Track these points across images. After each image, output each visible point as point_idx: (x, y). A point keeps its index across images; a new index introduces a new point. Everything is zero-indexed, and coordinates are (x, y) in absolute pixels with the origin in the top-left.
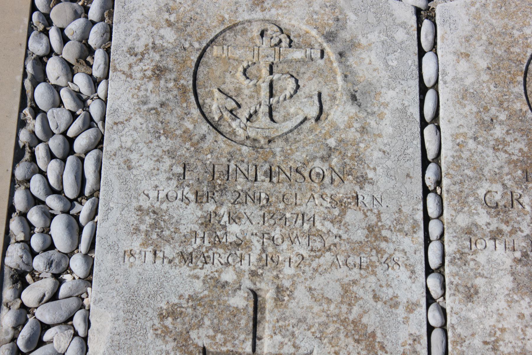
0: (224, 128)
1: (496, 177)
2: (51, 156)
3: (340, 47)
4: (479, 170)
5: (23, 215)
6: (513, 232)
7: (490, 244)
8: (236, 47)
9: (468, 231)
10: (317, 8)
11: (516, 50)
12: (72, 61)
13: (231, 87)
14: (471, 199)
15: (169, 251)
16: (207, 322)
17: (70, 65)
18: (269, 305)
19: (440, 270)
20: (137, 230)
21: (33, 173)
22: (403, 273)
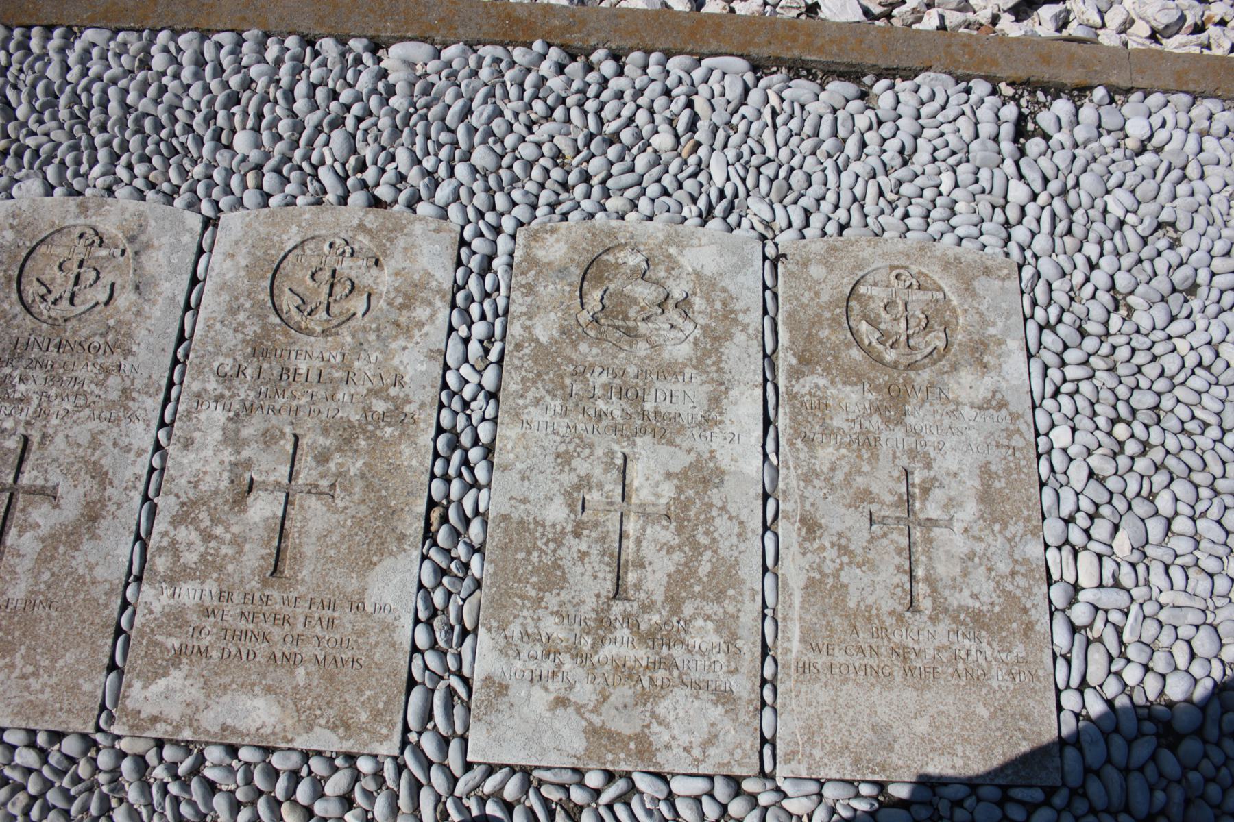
0: (35, 310)
1: (231, 353)
3: (137, 246)
4: (218, 347)
6: (232, 396)
7: (213, 405)
9: (198, 395)
13: (48, 277)
14: (207, 369)
18: (35, 447)
22: (140, 426)
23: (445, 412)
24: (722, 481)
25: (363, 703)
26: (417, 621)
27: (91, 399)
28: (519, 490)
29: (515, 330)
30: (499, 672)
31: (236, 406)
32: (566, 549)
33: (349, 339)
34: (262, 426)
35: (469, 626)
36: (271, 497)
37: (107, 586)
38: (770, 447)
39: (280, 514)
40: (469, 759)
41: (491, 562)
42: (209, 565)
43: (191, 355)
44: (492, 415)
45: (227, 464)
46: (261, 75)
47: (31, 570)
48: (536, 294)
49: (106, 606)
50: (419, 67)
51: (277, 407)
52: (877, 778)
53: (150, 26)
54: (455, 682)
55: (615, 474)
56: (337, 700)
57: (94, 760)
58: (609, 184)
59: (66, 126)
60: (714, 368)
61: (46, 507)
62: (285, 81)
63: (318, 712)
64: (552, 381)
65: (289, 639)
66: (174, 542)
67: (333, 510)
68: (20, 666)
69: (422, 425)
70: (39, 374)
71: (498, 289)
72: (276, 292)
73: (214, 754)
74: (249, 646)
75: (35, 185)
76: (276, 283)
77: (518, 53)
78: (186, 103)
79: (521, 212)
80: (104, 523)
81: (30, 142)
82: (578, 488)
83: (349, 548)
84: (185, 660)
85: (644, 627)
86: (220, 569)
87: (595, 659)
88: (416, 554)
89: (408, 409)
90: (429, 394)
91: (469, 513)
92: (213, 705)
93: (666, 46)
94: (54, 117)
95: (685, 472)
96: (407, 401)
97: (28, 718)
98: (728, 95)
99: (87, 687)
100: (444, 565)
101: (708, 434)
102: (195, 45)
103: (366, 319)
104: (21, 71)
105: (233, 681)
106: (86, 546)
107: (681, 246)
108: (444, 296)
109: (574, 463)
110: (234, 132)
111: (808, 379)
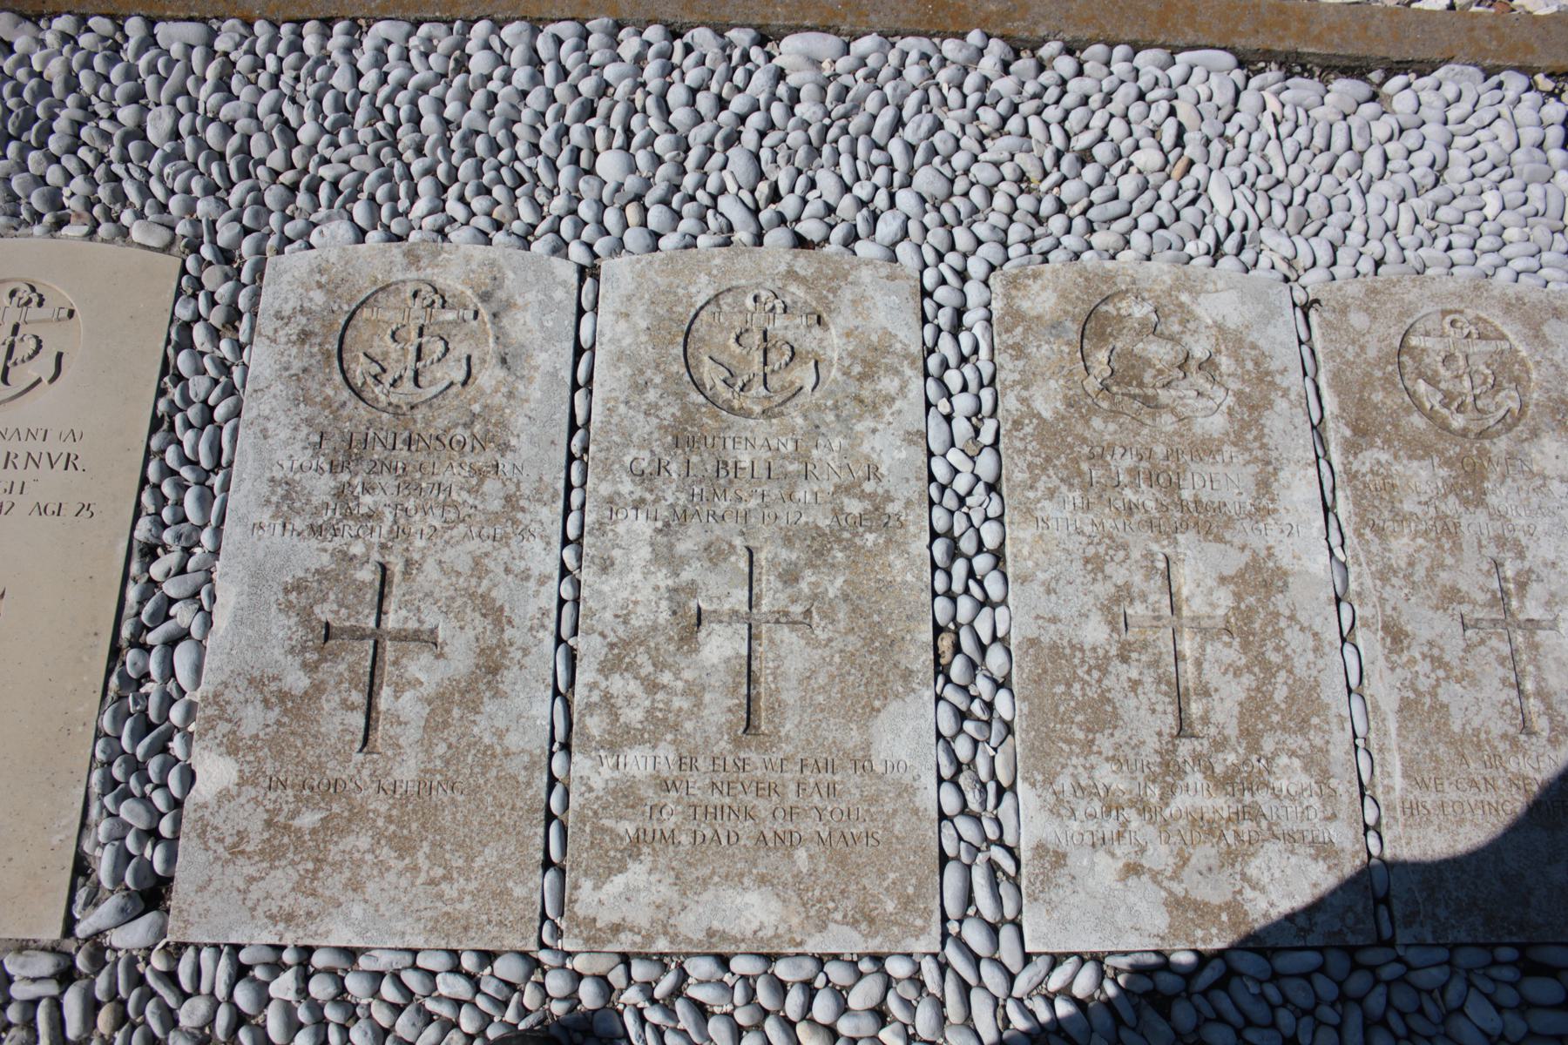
0: (367, 395)
1: (645, 443)
2: (188, 425)
3: (494, 306)
4: (627, 436)
5: (157, 487)
6: (657, 501)
7: (632, 513)
8: (387, 308)
9: (610, 501)
10: (474, 267)
11: (679, 309)
12: (219, 326)
13: (378, 351)
14: (616, 466)
15: (299, 523)
16: (332, 596)
17: (217, 330)
18: (397, 578)
19: (579, 540)
20: (268, 501)
21: (170, 443)
22: (537, 545)
23: (937, 511)
24: (1286, 584)
25: (887, 889)
26: (940, 780)
27: (464, 511)
28: (1046, 606)
29: (1010, 403)
30: (1052, 838)
31: (664, 513)
32: (1113, 678)
33: (800, 421)
34: (704, 539)
35: (1005, 783)
36: (730, 630)
37: (526, 758)
38: (1335, 539)
39: (745, 652)
40: (1028, 950)
41: (1025, 699)
42: (659, 725)
43: (592, 448)
44: (998, 513)
45: (663, 590)
46: (622, 77)
47: (420, 742)
48: (1028, 356)
49: (529, 784)
50: (826, 65)
51: (719, 512)
52: (1515, 939)
53: (462, 15)
54: (998, 854)
55: (1158, 581)
56: (853, 887)
57: (542, 985)
58: (1092, 214)
59: (370, 149)
60: (1257, 444)
61: (426, 658)
62: (654, 85)
63: (831, 905)
64: (1065, 466)
65: (779, 813)
66: (607, 697)
67: (813, 643)
68: (425, 868)
69: (912, 529)
70: (387, 480)
71: (976, 351)
72: (691, 361)
73: (700, 968)
74: (729, 825)
75: (342, 230)
76: (690, 351)
77: (950, 47)
78: (526, 115)
79: (990, 251)
80: (509, 675)
81: (325, 172)
82: (1117, 600)
83: (842, 691)
84: (645, 850)
85: (1219, 769)
86: (676, 727)
87: (1167, 813)
88: (928, 695)
89: (891, 508)
90: (915, 487)
91: (986, 639)
92: (692, 905)
93: (1132, 37)
94: (353, 138)
95: (1241, 574)
96: (888, 498)
97: (447, 935)
98: (1217, 100)
99: (519, 891)
100: (963, 707)
101: (1261, 526)
102: (526, 36)
103: (817, 394)
104: (297, 79)
105: (713, 873)
106: (489, 707)
107: (1195, 293)
108: (913, 363)
109: (1109, 569)
110: (596, 154)
111: (1368, 453)
